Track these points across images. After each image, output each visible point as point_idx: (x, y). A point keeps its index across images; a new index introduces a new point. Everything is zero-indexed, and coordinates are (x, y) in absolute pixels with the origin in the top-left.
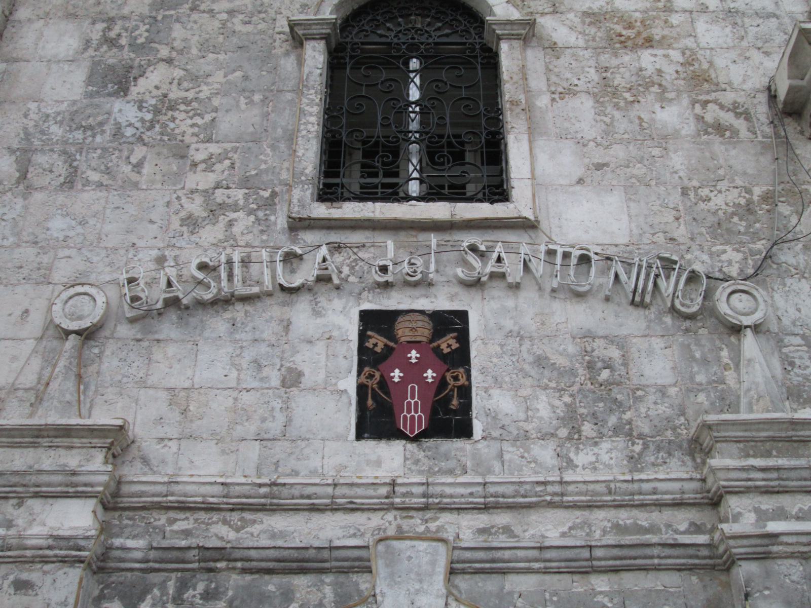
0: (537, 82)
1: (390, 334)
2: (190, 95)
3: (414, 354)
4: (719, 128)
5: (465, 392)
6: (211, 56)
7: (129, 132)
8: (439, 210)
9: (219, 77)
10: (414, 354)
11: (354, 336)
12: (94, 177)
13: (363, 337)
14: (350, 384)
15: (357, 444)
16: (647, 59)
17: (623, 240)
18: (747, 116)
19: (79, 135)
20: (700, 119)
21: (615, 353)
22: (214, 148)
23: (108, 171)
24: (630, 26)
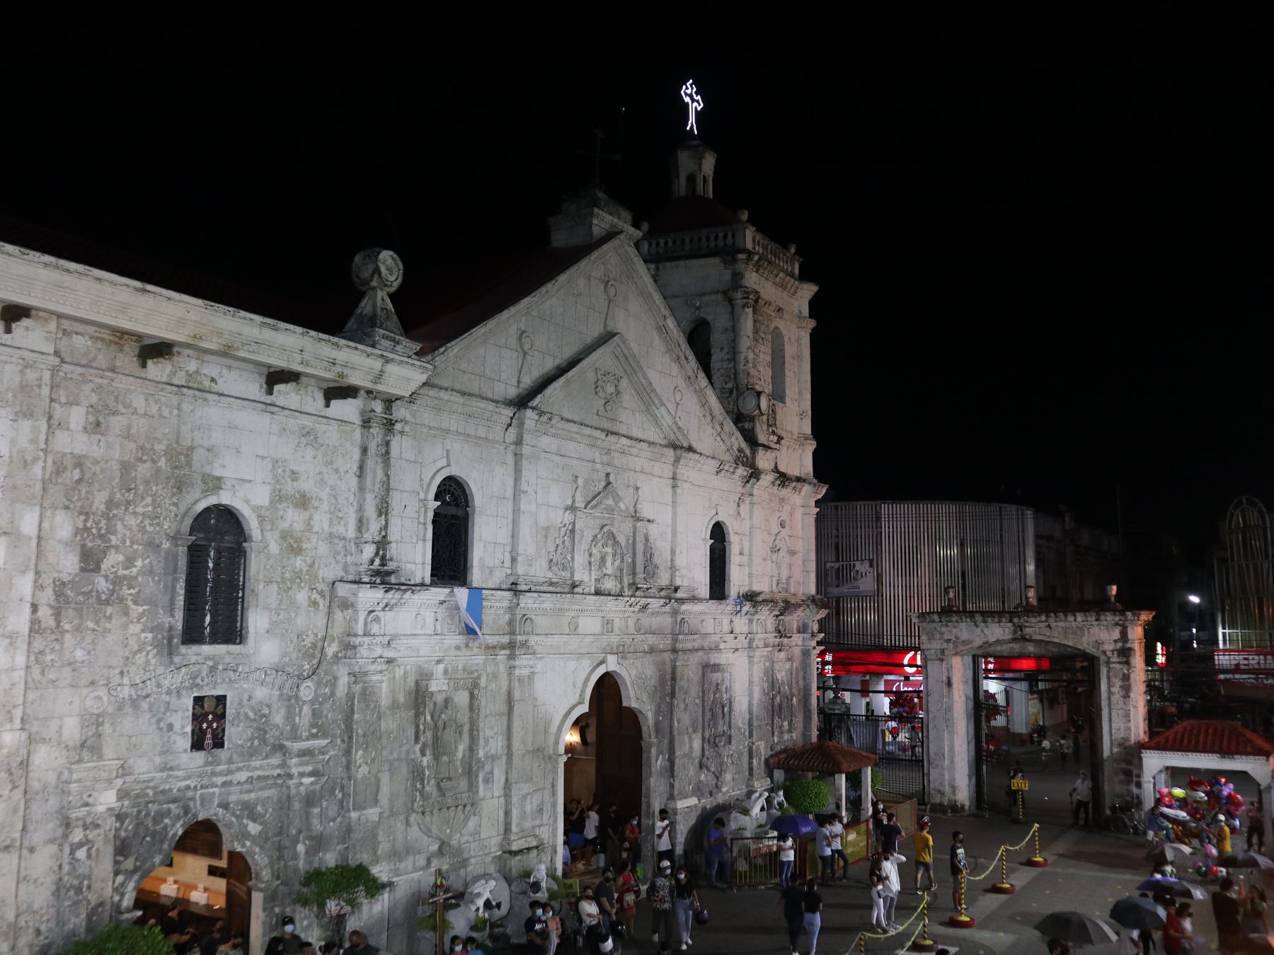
0: (261, 577)
1: (202, 707)
2: (127, 572)
3: (210, 717)
4: (315, 603)
5: (223, 730)
6: (135, 547)
7: (104, 597)
8: (221, 649)
9: (139, 563)
10: (210, 717)
11: (191, 708)
12: (91, 625)
13: (194, 708)
14: (189, 729)
15: (190, 754)
16: (299, 563)
17: (276, 660)
18: (323, 597)
19: (81, 598)
20: (309, 597)
21: (266, 711)
22: (140, 609)
23: (97, 622)
24: (295, 542)
